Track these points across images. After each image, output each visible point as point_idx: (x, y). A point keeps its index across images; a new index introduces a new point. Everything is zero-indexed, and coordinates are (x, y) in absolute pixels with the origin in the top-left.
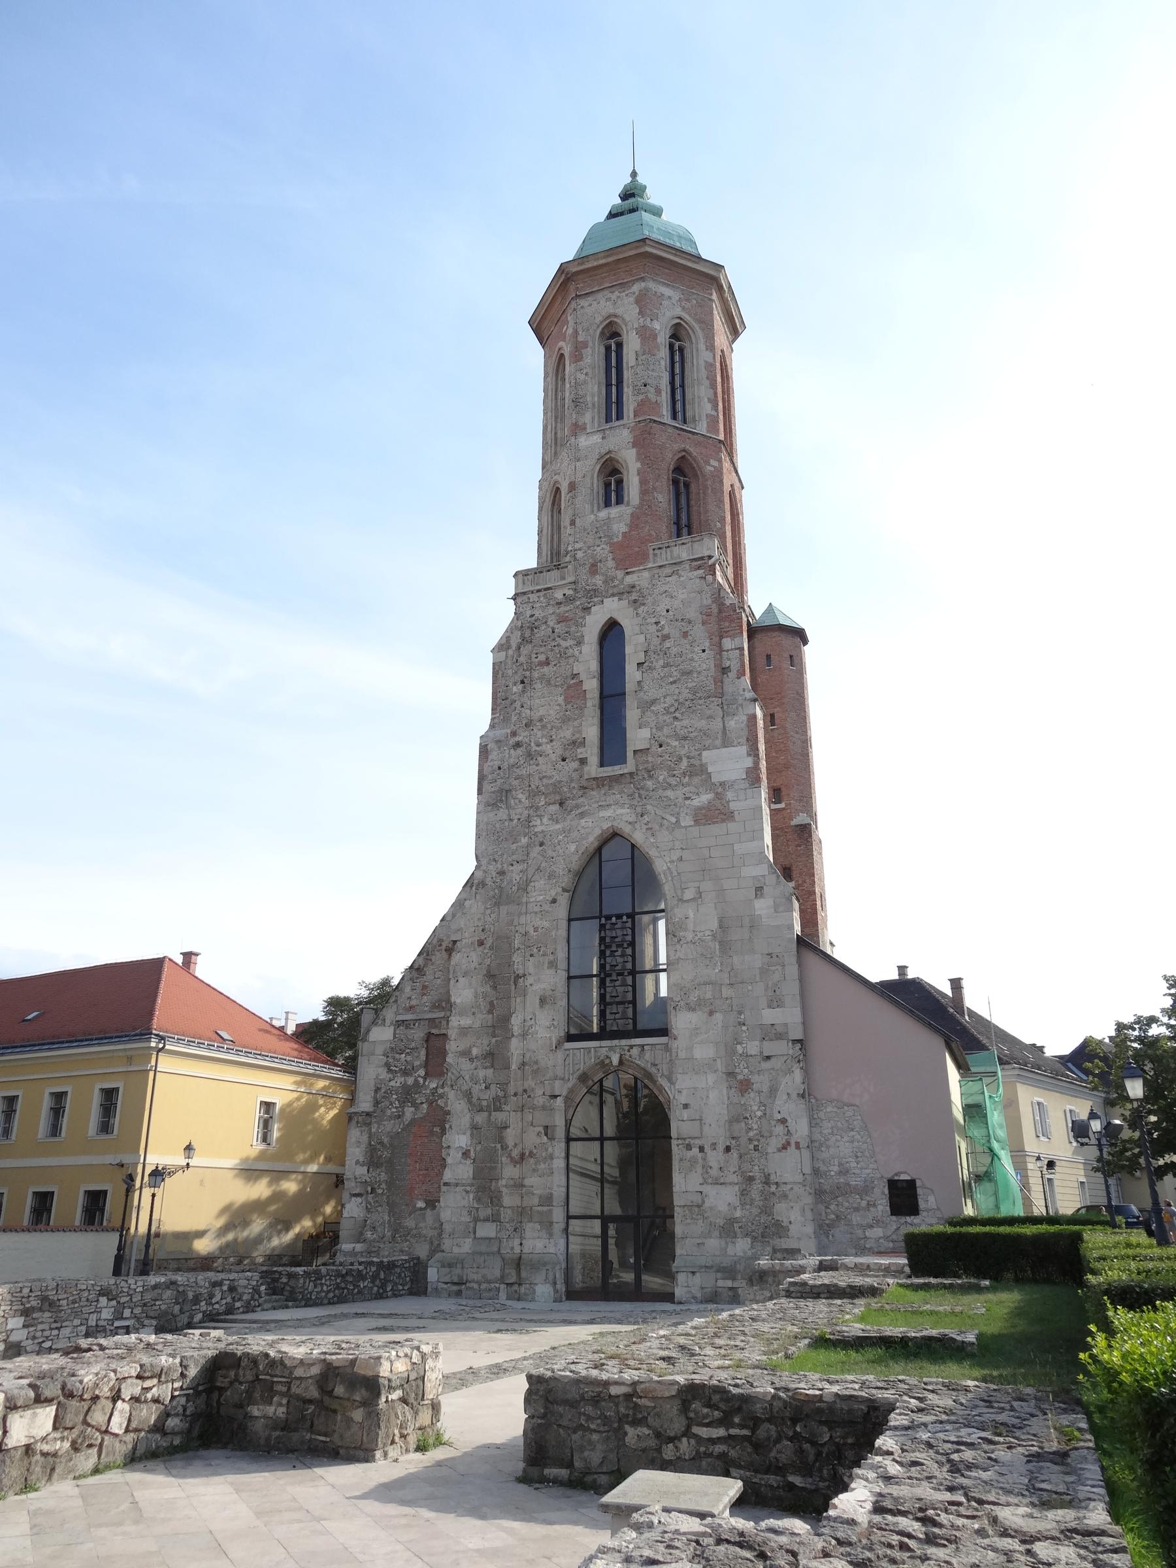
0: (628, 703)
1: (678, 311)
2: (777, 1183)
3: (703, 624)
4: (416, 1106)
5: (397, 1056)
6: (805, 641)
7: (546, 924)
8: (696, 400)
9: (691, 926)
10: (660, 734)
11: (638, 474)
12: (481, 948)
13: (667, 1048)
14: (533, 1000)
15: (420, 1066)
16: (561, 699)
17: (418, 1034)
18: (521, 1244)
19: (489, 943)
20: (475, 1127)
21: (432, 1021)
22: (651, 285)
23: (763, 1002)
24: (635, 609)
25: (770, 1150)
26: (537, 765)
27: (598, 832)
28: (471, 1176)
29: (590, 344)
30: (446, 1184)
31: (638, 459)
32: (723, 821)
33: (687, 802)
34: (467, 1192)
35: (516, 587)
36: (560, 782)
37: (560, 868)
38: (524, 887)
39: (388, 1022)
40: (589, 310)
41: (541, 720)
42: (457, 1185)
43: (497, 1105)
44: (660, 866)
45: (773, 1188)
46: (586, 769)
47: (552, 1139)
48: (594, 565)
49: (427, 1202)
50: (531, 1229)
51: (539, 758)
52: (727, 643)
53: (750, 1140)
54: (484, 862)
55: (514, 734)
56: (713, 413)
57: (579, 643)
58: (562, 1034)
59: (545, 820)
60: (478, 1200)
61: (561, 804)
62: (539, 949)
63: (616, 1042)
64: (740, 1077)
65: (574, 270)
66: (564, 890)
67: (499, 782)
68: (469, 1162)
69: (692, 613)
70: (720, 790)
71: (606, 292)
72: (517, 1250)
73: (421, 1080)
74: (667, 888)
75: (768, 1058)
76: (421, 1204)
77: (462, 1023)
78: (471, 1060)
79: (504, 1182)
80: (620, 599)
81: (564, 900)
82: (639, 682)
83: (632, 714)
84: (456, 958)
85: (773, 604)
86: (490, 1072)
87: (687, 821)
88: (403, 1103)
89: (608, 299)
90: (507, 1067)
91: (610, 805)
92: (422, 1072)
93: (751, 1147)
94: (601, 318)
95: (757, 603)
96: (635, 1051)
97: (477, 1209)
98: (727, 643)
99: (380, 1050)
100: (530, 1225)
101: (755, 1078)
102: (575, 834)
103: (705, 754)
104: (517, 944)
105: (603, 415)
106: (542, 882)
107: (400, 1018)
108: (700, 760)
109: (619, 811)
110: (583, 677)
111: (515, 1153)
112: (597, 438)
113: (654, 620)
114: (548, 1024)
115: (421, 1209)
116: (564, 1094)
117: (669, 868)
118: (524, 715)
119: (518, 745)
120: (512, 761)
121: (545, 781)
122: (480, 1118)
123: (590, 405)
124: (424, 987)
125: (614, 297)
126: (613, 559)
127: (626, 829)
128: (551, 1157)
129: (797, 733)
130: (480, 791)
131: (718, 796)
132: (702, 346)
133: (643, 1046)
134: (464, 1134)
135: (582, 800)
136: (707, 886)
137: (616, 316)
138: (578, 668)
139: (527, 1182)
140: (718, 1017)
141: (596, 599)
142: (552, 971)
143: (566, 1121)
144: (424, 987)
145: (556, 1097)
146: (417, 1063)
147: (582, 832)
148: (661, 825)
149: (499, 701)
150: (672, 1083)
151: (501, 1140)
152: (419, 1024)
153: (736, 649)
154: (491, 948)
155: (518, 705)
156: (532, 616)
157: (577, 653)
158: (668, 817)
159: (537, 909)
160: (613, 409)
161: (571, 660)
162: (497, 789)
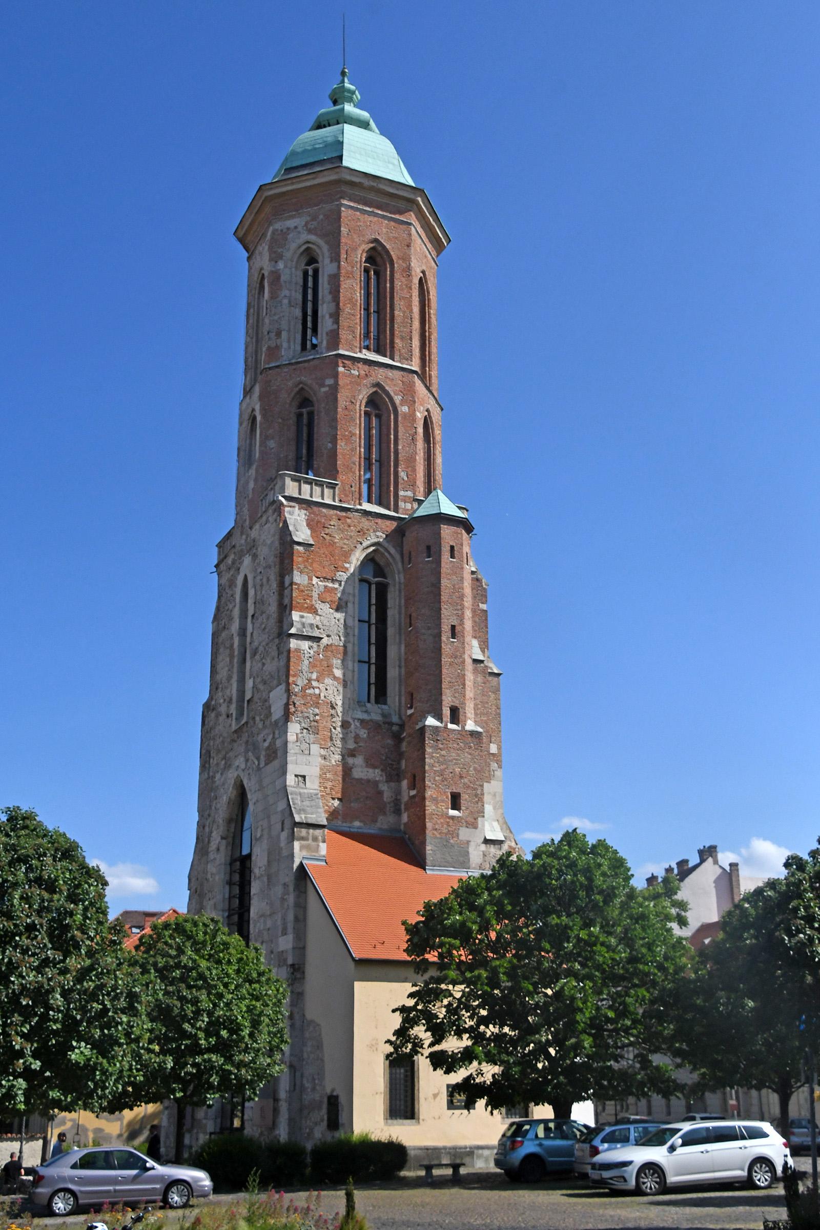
1: (305, 236)
22: (278, 226)
56: (335, 327)
66: (222, 838)
129: (429, 628)
132: (327, 261)
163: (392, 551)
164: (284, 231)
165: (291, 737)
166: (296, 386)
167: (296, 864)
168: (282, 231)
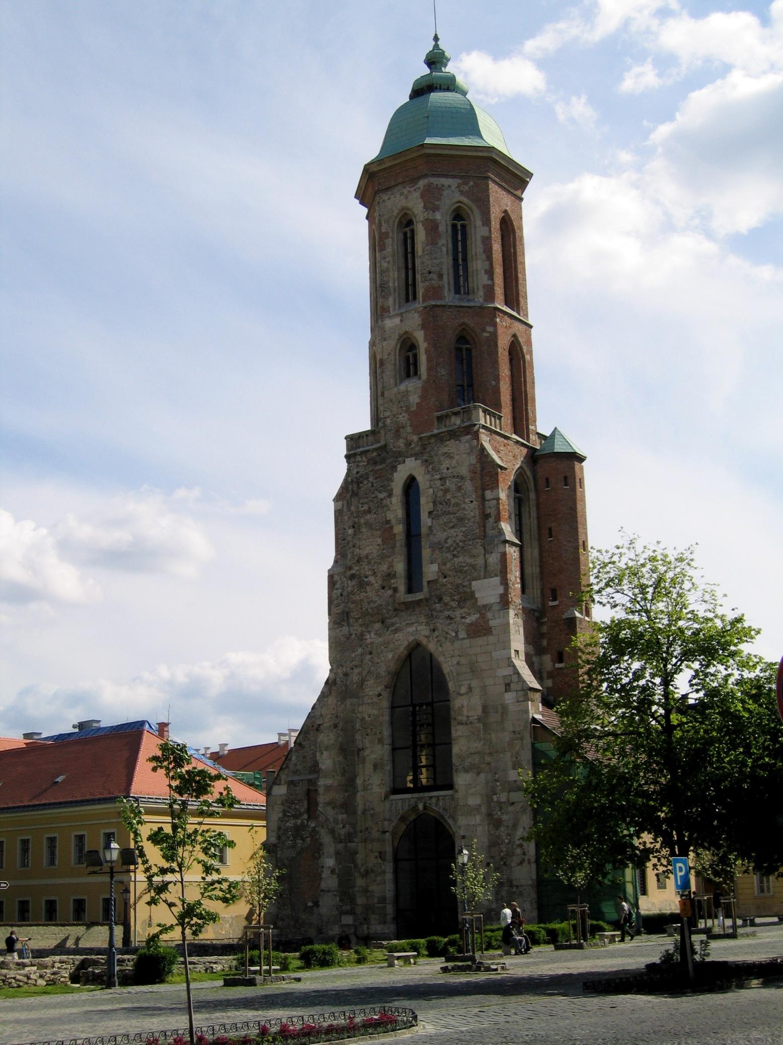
0: (423, 544)
2: (517, 886)
3: (471, 480)
4: (303, 839)
6: (581, 459)
7: (376, 712)
8: (475, 273)
9: (465, 712)
10: (444, 567)
11: (426, 353)
12: (335, 730)
13: (452, 797)
14: (369, 767)
16: (379, 541)
17: (301, 790)
18: (368, 928)
19: (340, 726)
20: (337, 854)
21: (310, 781)
23: (510, 764)
24: (427, 467)
25: (513, 865)
26: (366, 592)
27: (406, 643)
28: (337, 884)
29: (391, 235)
30: (322, 891)
31: (426, 340)
32: (485, 635)
33: (463, 620)
34: (335, 896)
35: (348, 449)
36: (381, 605)
37: (382, 670)
38: (362, 684)
39: (283, 782)
40: (389, 204)
41: (367, 557)
42: (329, 891)
43: (350, 837)
44: (446, 668)
45: (514, 889)
46: (398, 595)
47: (384, 860)
48: (398, 431)
49: (313, 902)
50: (373, 918)
51: (368, 587)
52: (489, 494)
53: (502, 859)
54: (335, 666)
55: (350, 568)
56: (490, 282)
57: (390, 495)
58: (388, 789)
59: (372, 635)
60: (341, 900)
61: (383, 622)
62: (371, 729)
63: (421, 794)
64: (496, 817)
65: (375, 169)
66: (386, 687)
67: (342, 605)
68: (335, 876)
69: (464, 471)
70: (483, 611)
71: (400, 187)
72: (366, 932)
73: (306, 822)
74: (451, 685)
75: (513, 804)
76: (310, 904)
77: (326, 782)
79: (356, 889)
80: (416, 459)
81: (385, 694)
82: (430, 527)
83: (426, 553)
84: (322, 737)
85: (559, 429)
86: (345, 816)
87: (462, 635)
88: (295, 838)
89: (402, 194)
90: (355, 813)
91: (414, 623)
92: (306, 816)
93: (502, 863)
94: (397, 211)
95: (543, 426)
96: (434, 800)
97: (341, 906)
98: (489, 494)
99: (279, 802)
100: (373, 916)
101: (505, 817)
102: (392, 646)
103: (474, 583)
105: (403, 296)
106: (372, 681)
107: (289, 779)
108: (471, 588)
109: (419, 628)
110: (393, 522)
111: (362, 870)
112: (397, 320)
113: (438, 477)
114: (379, 783)
115: (310, 907)
116: (391, 829)
117: (451, 671)
118: (355, 553)
119: (352, 577)
120: (350, 589)
121: (372, 605)
122: (340, 846)
123: (392, 290)
125: (405, 191)
126: (411, 426)
127: (424, 641)
128: (384, 872)
129: (569, 542)
130: (330, 614)
131: (483, 616)
132: (479, 223)
133: (438, 797)
134: (331, 858)
135: (395, 619)
136: (474, 683)
137: (408, 209)
138: (390, 516)
139: (371, 888)
140: (482, 775)
141: (400, 459)
142: (380, 746)
143: (393, 848)
145: (384, 832)
146: (302, 810)
147: (396, 643)
148: (446, 638)
149: (340, 541)
150: (455, 820)
151: (353, 861)
153: (494, 499)
154: (342, 730)
155: (351, 545)
156: (357, 473)
157: (389, 503)
158: (450, 632)
159: (370, 701)
160: (409, 293)
161: (385, 508)
162: (339, 611)
163: (529, 473)
164: (439, 186)
165: (511, 621)
166: (460, 326)
167: (531, 717)
168: (437, 185)
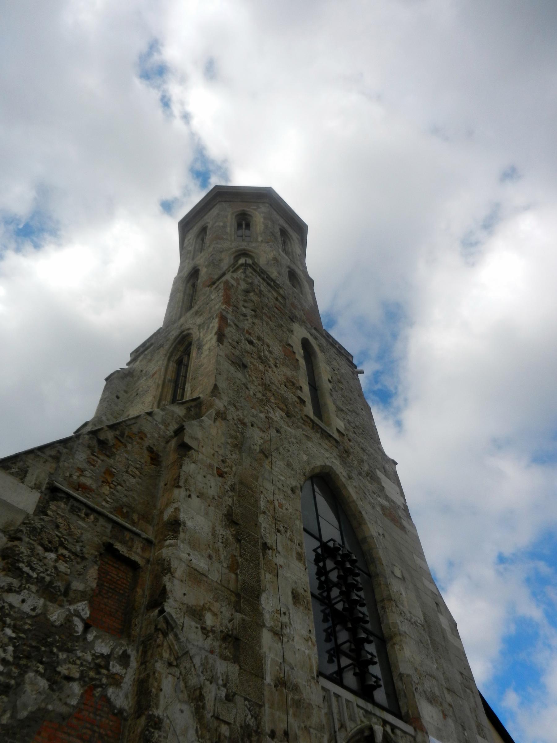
5: (40, 549)
15: (83, 596)
19: (231, 480)
39: (31, 479)
73: (80, 627)
78: (205, 631)
104: (262, 504)
119: (251, 343)
124: (109, 472)
144: (109, 472)
152: (96, 520)
